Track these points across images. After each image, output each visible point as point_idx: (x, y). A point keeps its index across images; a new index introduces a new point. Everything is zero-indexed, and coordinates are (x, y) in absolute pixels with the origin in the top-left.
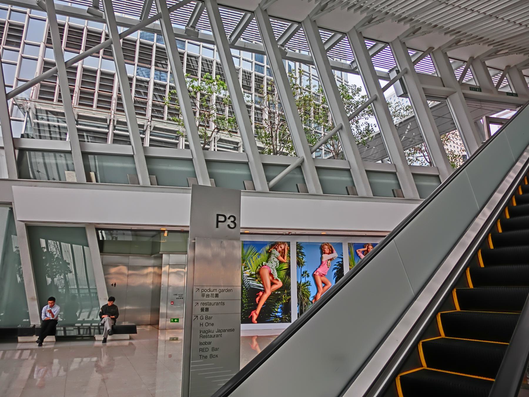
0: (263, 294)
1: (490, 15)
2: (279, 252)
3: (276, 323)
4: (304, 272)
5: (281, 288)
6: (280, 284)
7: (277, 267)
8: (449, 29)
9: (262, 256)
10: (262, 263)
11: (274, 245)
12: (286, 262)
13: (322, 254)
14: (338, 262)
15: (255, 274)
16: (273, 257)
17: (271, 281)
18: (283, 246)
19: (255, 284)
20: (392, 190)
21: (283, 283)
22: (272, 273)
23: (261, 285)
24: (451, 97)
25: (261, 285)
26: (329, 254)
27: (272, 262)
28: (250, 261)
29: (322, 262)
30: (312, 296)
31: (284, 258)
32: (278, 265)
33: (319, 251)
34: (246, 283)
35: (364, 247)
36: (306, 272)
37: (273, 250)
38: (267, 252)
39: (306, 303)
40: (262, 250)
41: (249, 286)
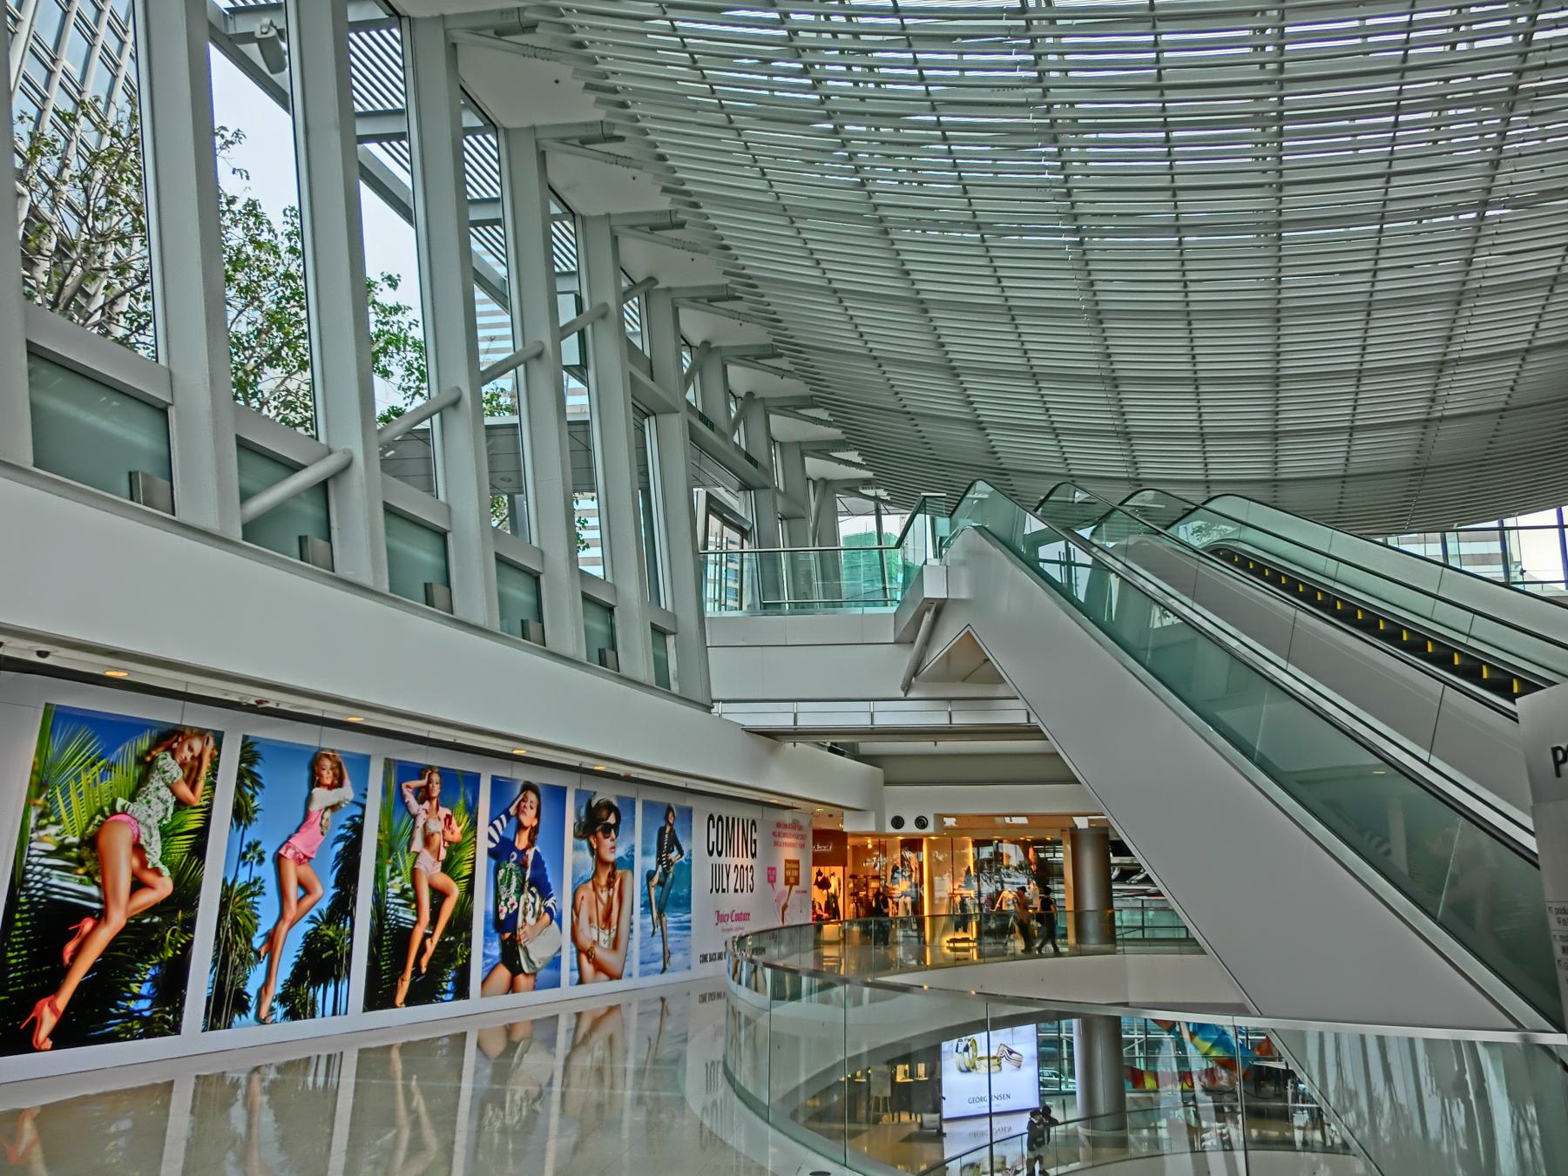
0: (94, 928)
1: (835, 291)
2: (182, 765)
3: (125, 1039)
4: (249, 846)
5: (167, 902)
6: (164, 887)
7: (165, 822)
8: (744, 269)
9: (119, 774)
10: (114, 801)
11: (169, 737)
12: (197, 804)
13: (312, 787)
14: (352, 818)
15: (79, 846)
16: (158, 781)
17: (134, 875)
18: (197, 745)
19: (71, 885)
20: (522, 621)
21: (176, 884)
22: (142, 842)
23: (94, 891)
24: (661, 418)
25: (94, 891)
26: (331, 787)
27: (148, 802)
28: (65, 791)
29: (307, 815)
30: (262, 930)
31: (193, 789)
32: (169, 816)
33: (306, 774)
34: (37, 882)
35: (421, 777)
36: (257, 844)
37: (162, 755)
38: (140, 760)
39: (240, 956)
40: (120, 749)
41: (48, 892)
